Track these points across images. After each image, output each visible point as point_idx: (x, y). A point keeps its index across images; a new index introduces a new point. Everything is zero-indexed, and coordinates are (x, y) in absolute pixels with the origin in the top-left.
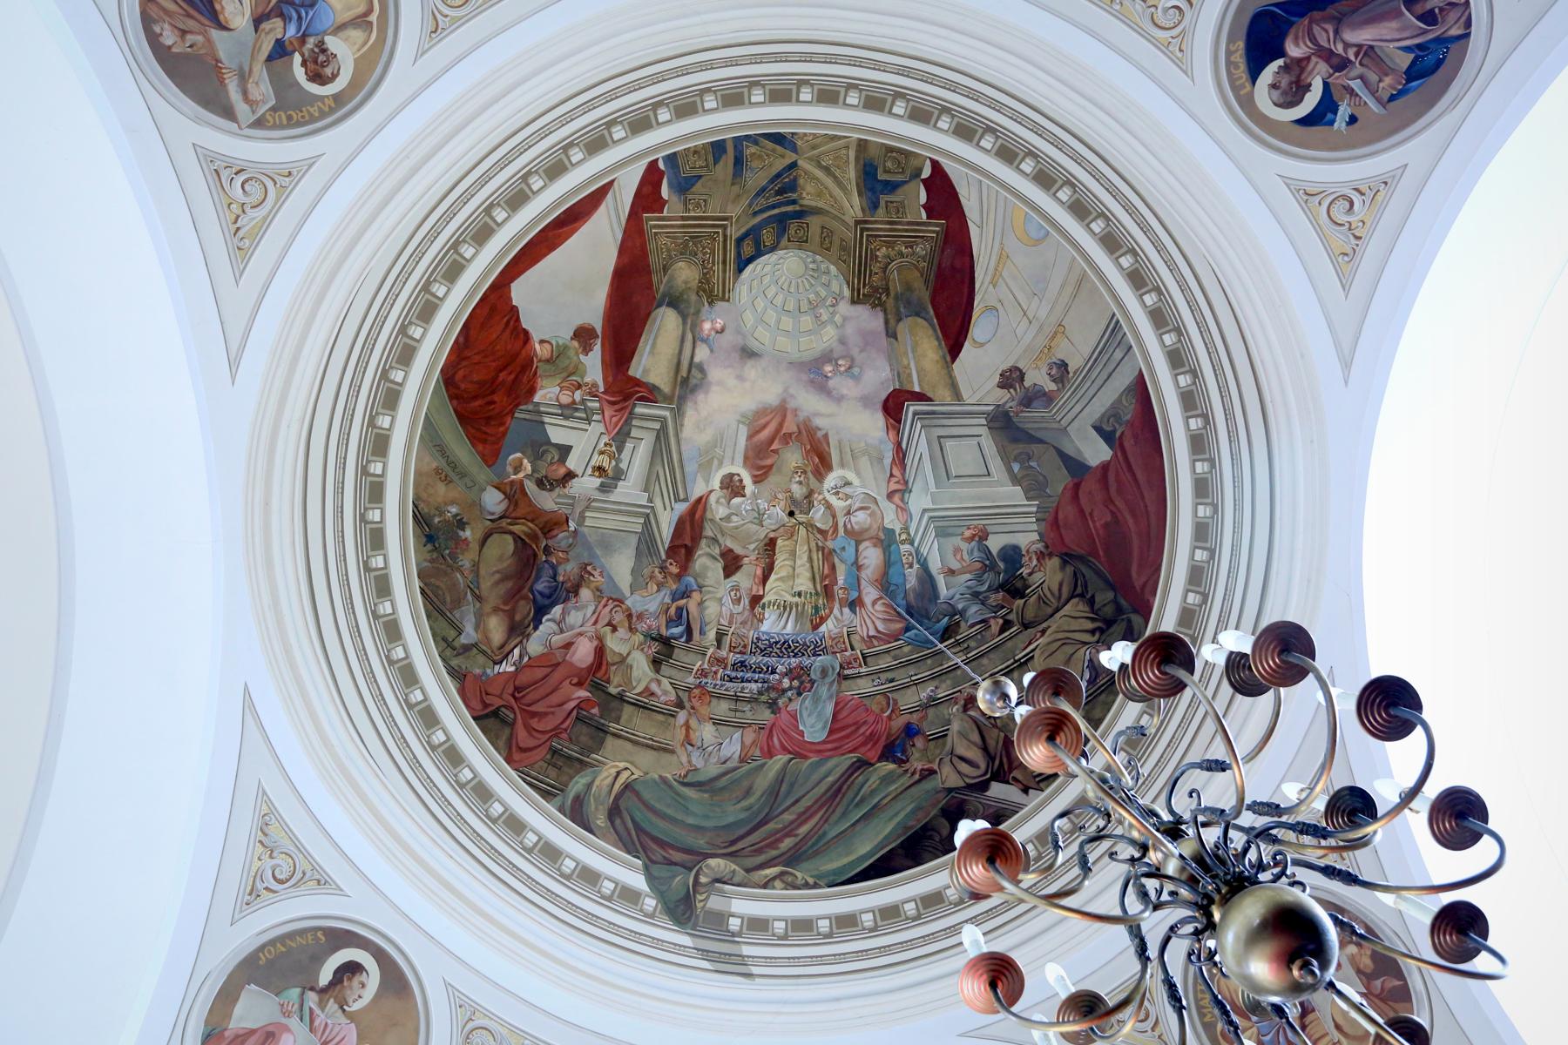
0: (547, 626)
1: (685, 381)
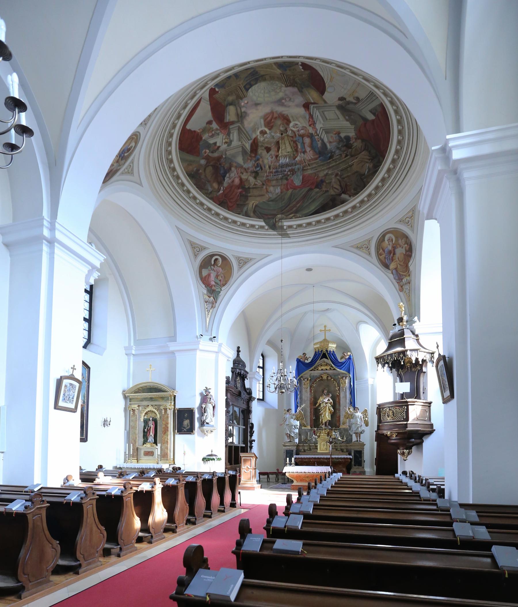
0: (226, 179)
1: (241, 116)
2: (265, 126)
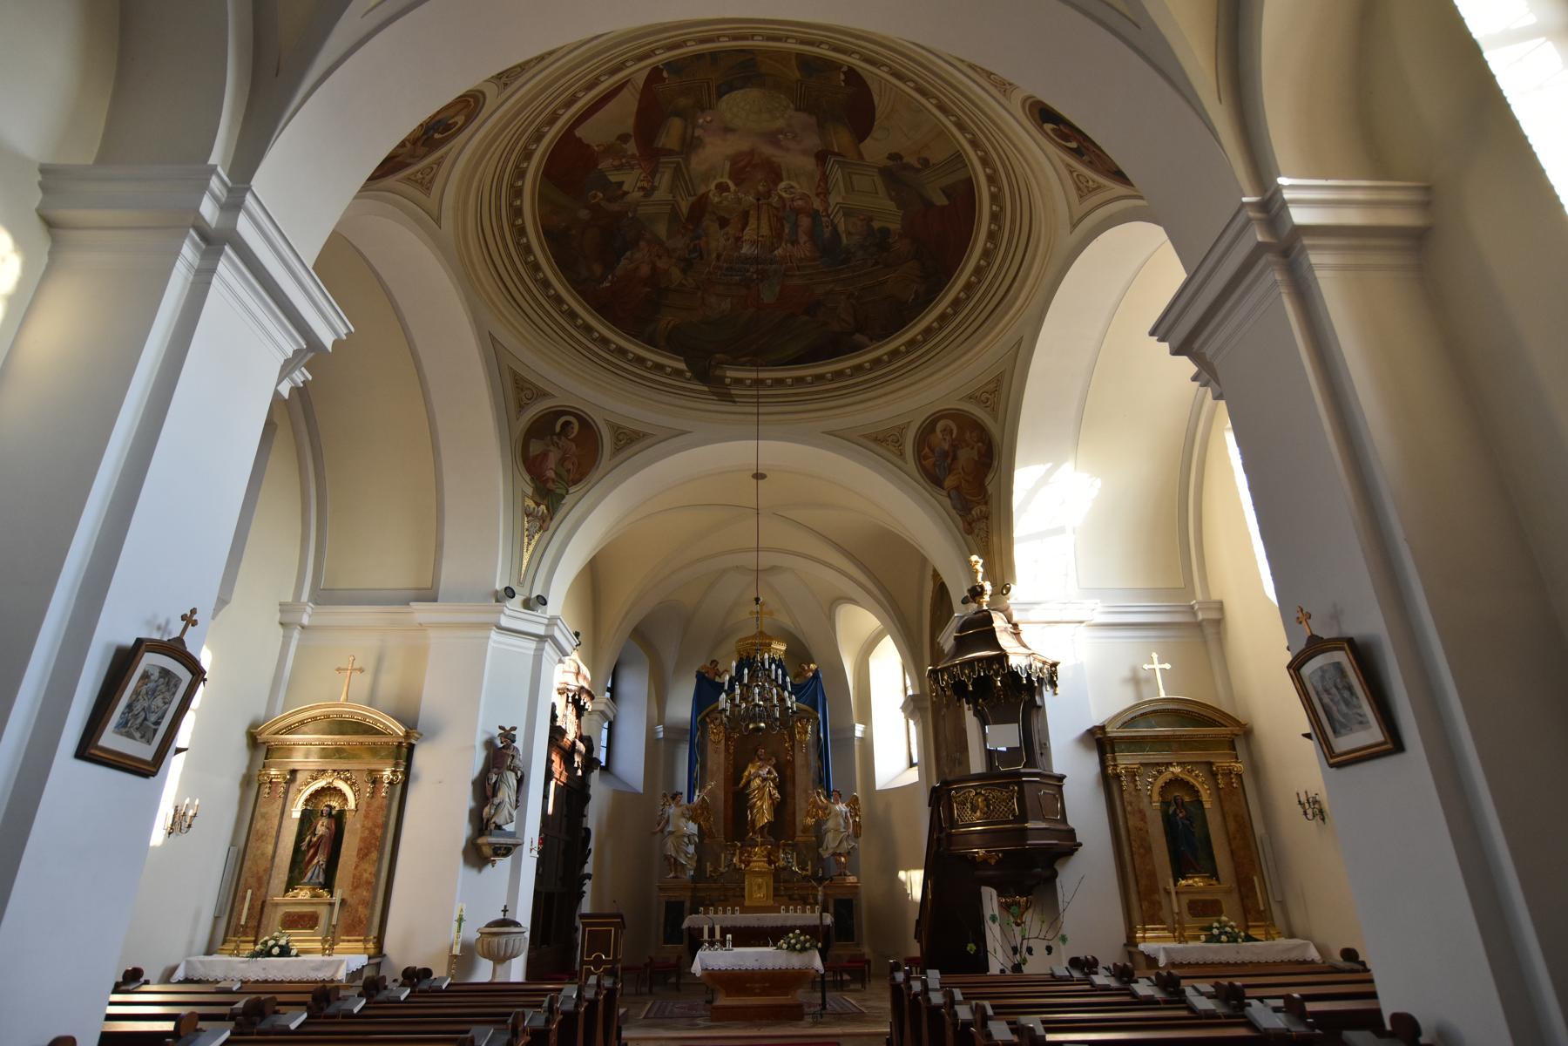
0: (623, 262)
2: (730, 178)
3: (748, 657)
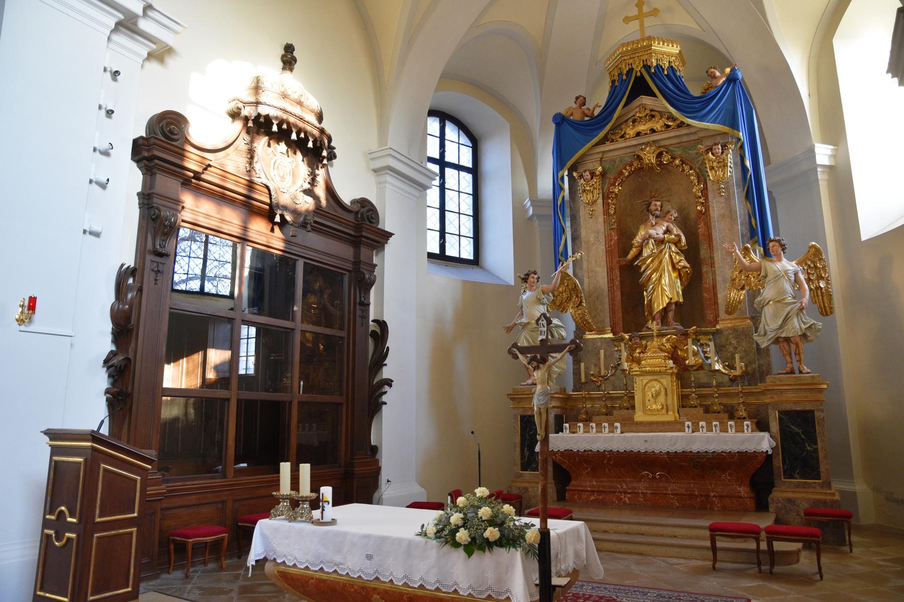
3: (620, 75)
